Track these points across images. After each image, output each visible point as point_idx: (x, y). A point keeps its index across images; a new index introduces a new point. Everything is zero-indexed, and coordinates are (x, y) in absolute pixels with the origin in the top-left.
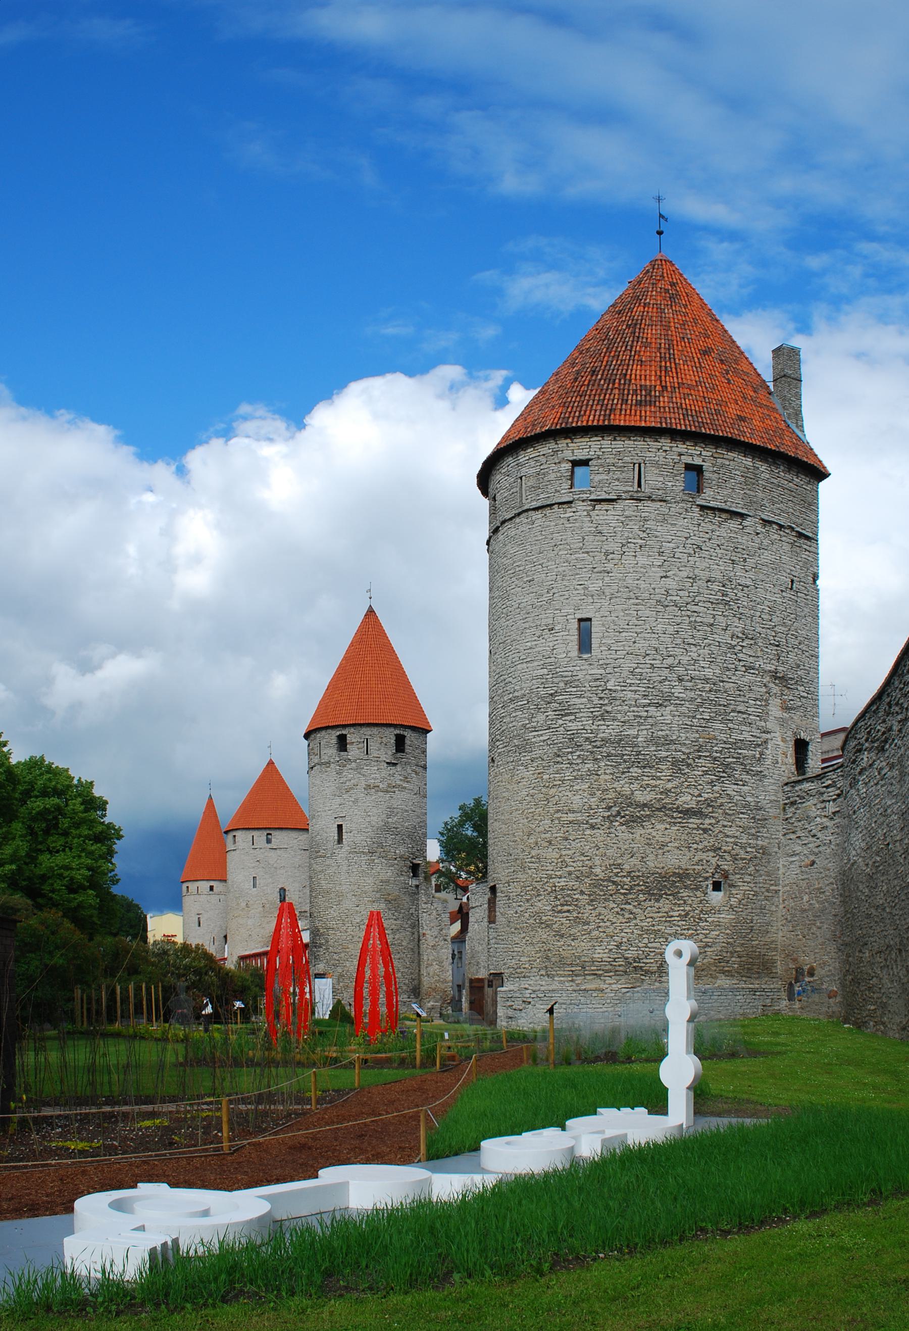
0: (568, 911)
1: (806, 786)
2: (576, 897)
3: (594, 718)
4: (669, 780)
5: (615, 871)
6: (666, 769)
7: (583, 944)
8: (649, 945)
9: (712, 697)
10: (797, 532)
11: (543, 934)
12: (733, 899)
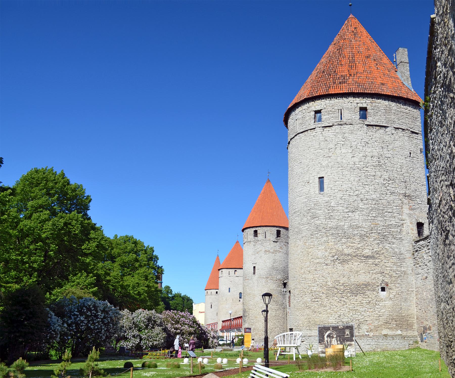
0: (317, 301)
1: (422, 243)
3: (326, 219)
4: (359, 244)
5: (337, 283)
6: (357, 239)
8: (353, 316)
9: (376, 207)
10: (411, 131)
11: (307, 311)
12: (391, 295)
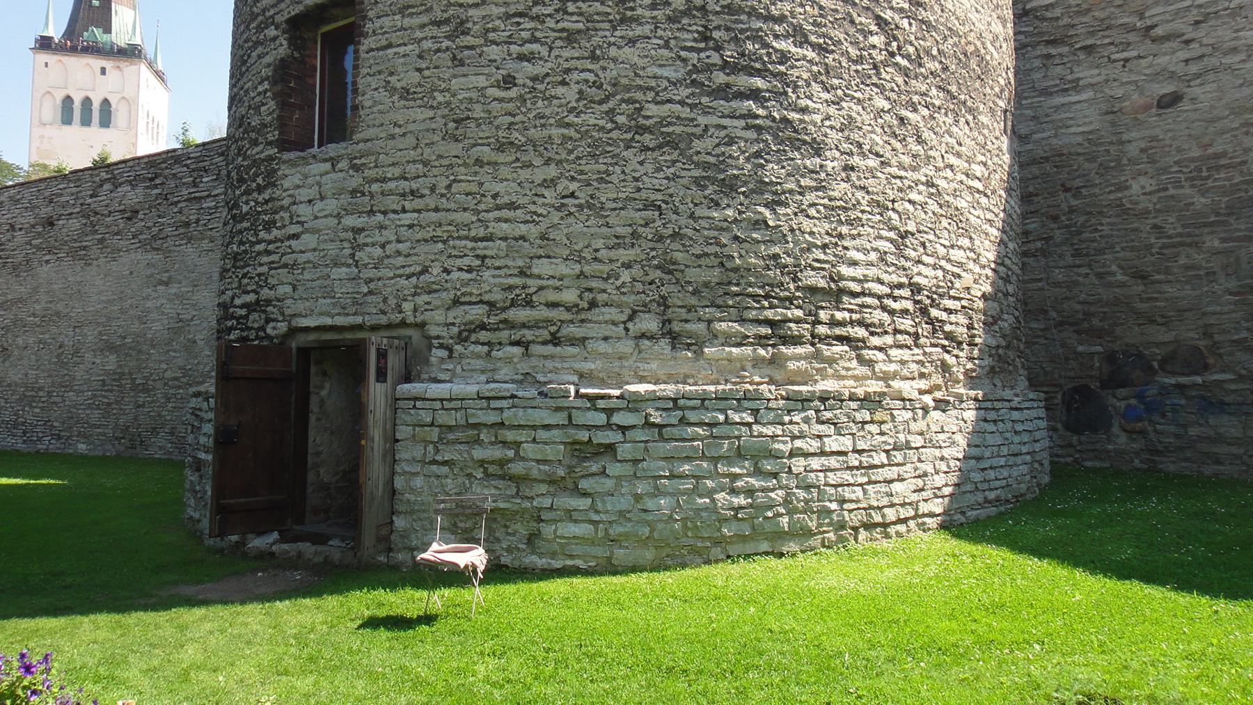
2: (781, 45)
7: (807, 225)
11: (647, 171)
